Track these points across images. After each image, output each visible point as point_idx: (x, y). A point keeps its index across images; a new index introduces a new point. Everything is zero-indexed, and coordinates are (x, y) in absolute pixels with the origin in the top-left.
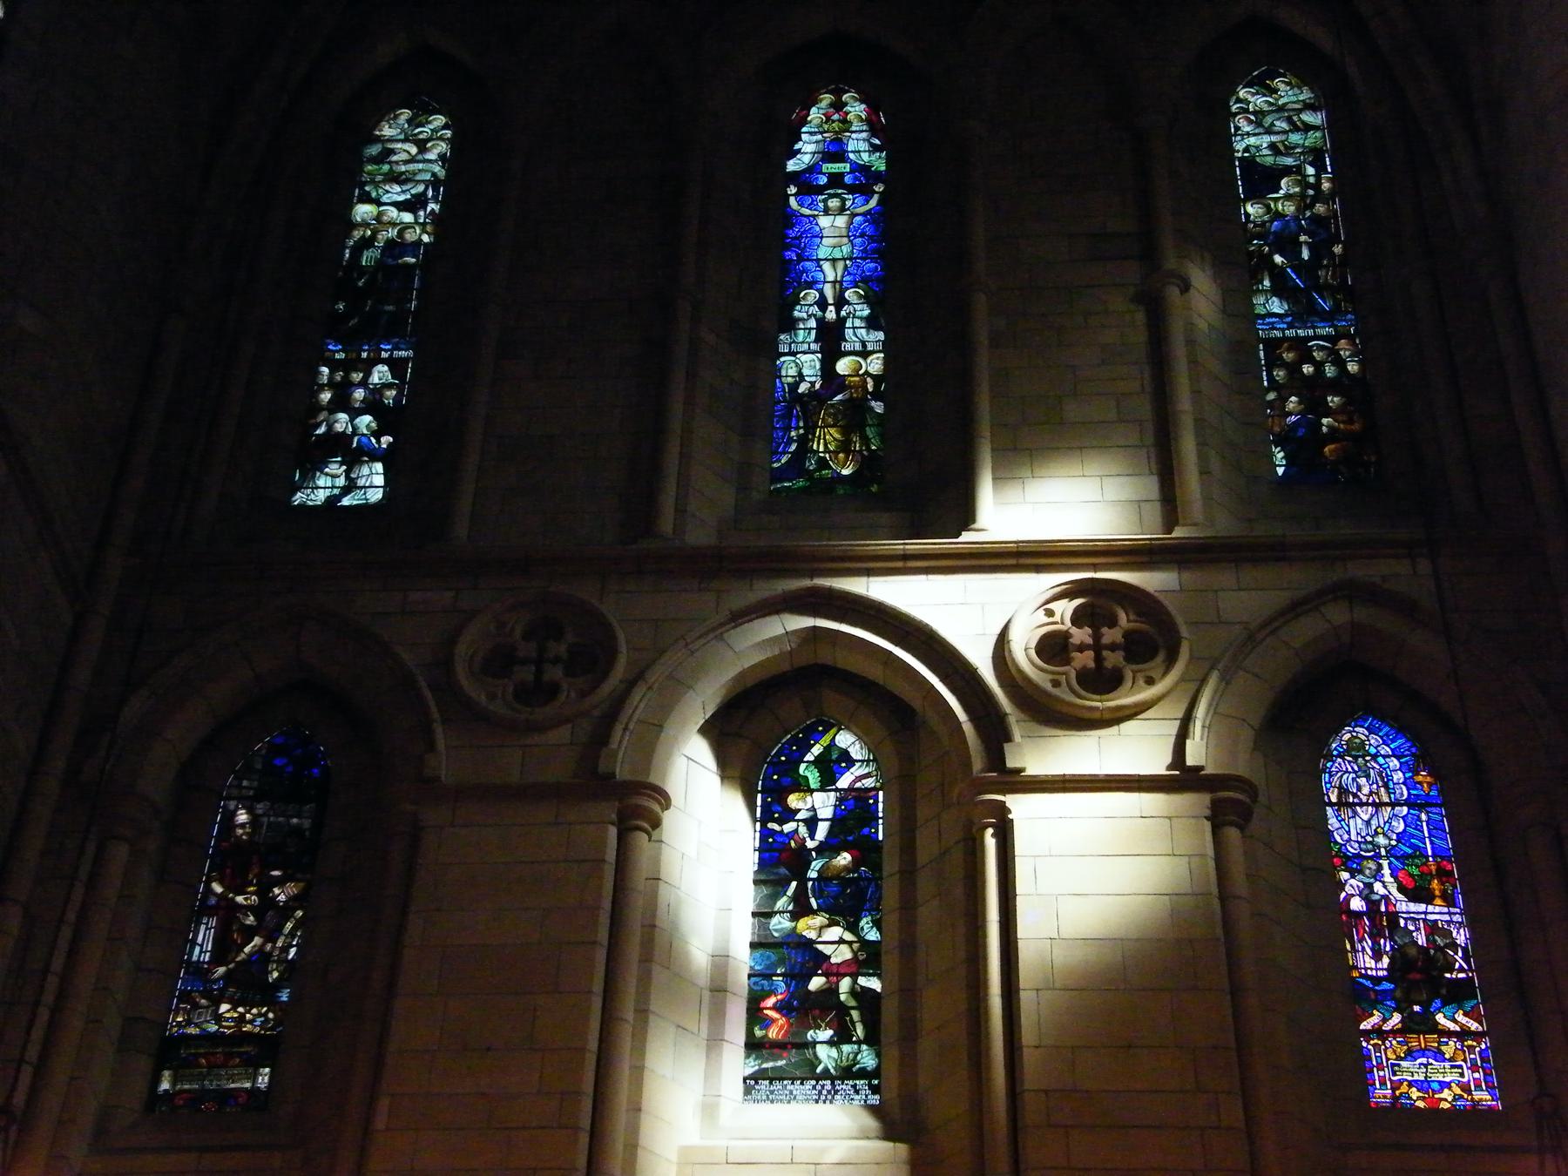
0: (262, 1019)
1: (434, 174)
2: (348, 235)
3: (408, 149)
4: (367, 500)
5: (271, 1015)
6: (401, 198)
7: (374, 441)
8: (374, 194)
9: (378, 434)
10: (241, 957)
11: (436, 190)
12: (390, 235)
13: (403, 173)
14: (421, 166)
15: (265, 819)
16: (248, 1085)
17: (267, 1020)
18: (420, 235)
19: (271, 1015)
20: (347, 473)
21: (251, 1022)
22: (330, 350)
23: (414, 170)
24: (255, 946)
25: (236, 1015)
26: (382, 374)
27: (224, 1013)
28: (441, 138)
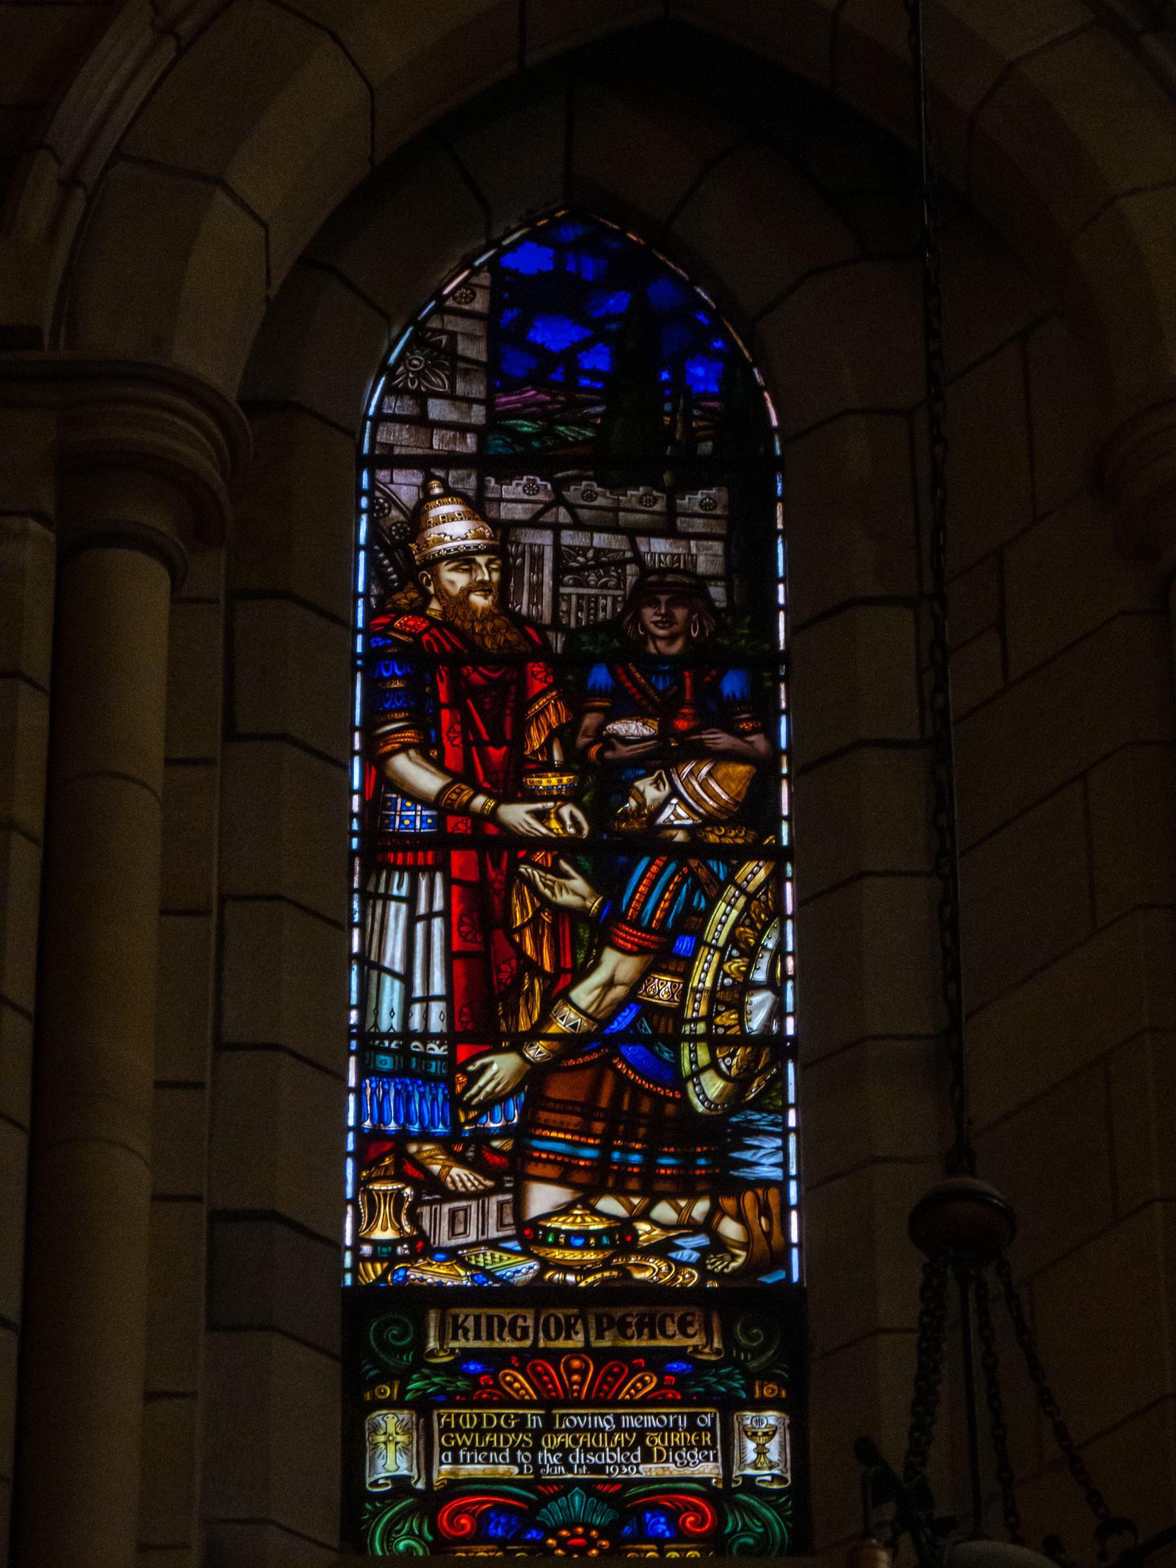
0: (702, 1240)
5: (730, 1229)
10: (565, 1021)
15: (545, 538)
16: (709, 1469)
17: (719, 1245)
19: (730, 1229)
21: (662, 1249)
24: (610, 984)
25: (596, 1225)
27: (547, 1216)
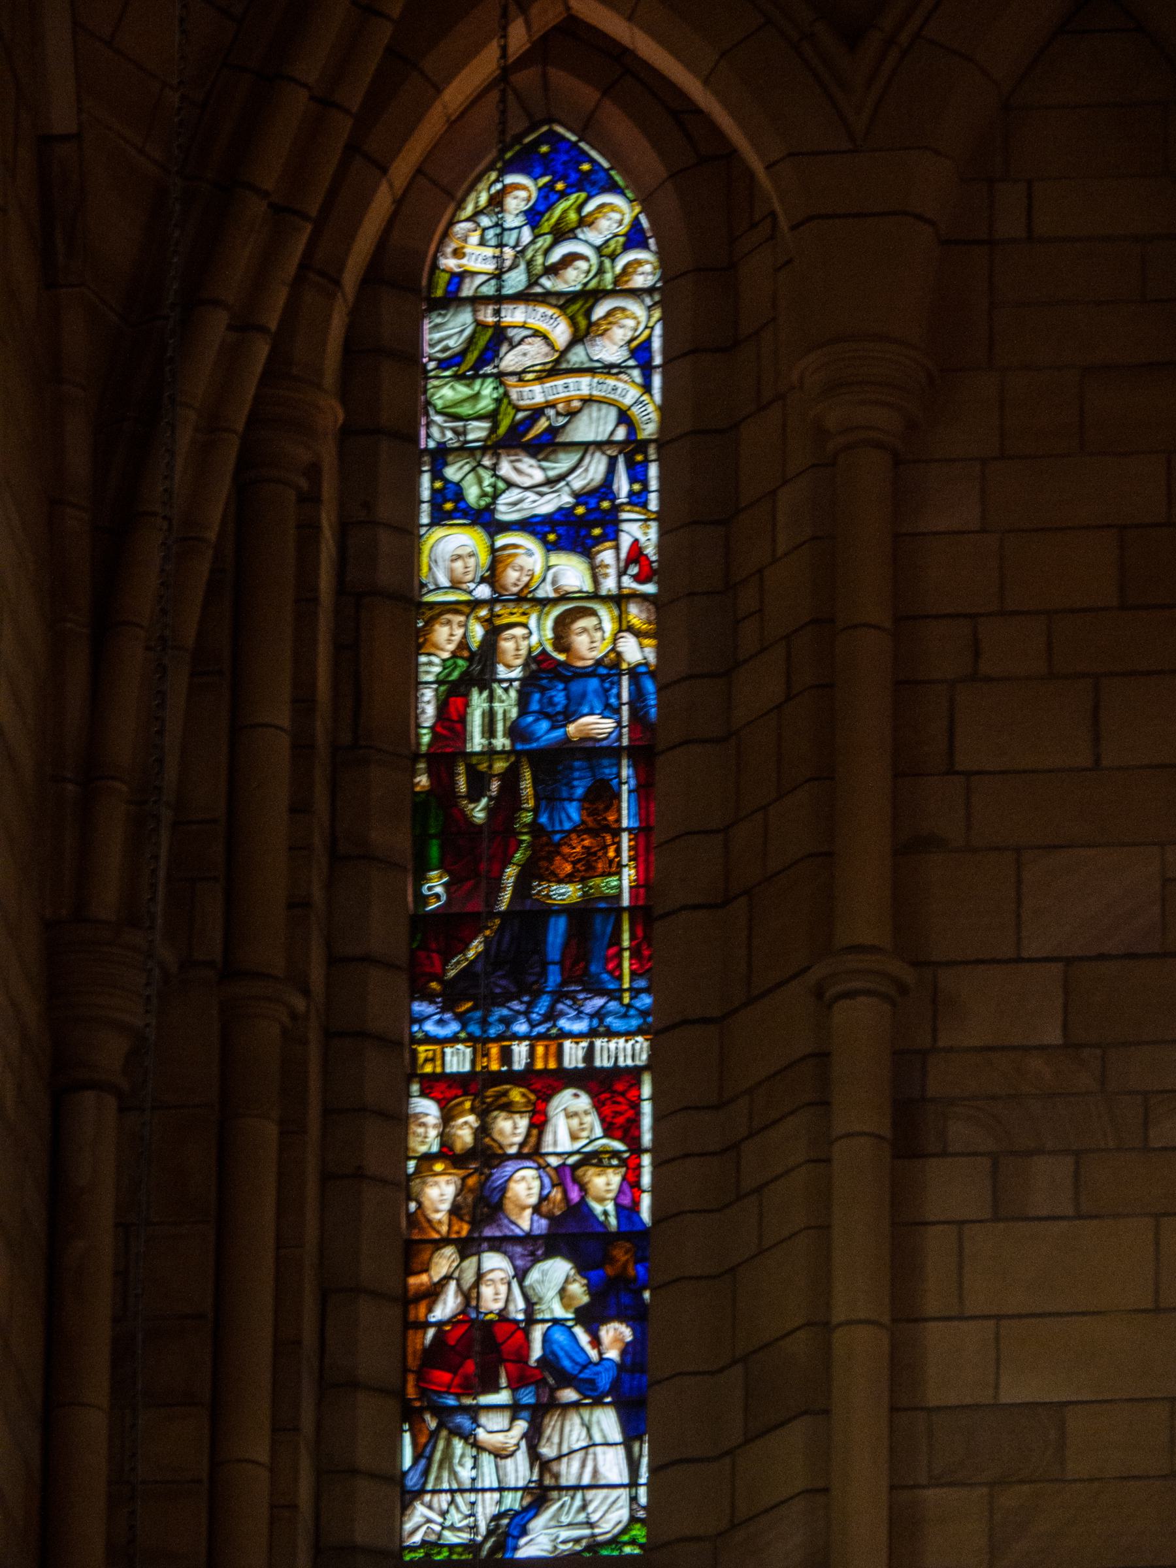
1: (624, 417)
2: (419, 642)
3: (542, 326)
4: (591, 1525)
6: (546, 505)
7: (583, 1338)
8: (472, 494)
9: (590, 1318)
11: (637, 474)
12: (534, 639)
13: (537, 412)
14: (584, 385)
18: (615, 640)
20: (533, 1438)
22: (429, 1039)
23: (568, 401)
26: (575, 1122)
28: (620, 290)
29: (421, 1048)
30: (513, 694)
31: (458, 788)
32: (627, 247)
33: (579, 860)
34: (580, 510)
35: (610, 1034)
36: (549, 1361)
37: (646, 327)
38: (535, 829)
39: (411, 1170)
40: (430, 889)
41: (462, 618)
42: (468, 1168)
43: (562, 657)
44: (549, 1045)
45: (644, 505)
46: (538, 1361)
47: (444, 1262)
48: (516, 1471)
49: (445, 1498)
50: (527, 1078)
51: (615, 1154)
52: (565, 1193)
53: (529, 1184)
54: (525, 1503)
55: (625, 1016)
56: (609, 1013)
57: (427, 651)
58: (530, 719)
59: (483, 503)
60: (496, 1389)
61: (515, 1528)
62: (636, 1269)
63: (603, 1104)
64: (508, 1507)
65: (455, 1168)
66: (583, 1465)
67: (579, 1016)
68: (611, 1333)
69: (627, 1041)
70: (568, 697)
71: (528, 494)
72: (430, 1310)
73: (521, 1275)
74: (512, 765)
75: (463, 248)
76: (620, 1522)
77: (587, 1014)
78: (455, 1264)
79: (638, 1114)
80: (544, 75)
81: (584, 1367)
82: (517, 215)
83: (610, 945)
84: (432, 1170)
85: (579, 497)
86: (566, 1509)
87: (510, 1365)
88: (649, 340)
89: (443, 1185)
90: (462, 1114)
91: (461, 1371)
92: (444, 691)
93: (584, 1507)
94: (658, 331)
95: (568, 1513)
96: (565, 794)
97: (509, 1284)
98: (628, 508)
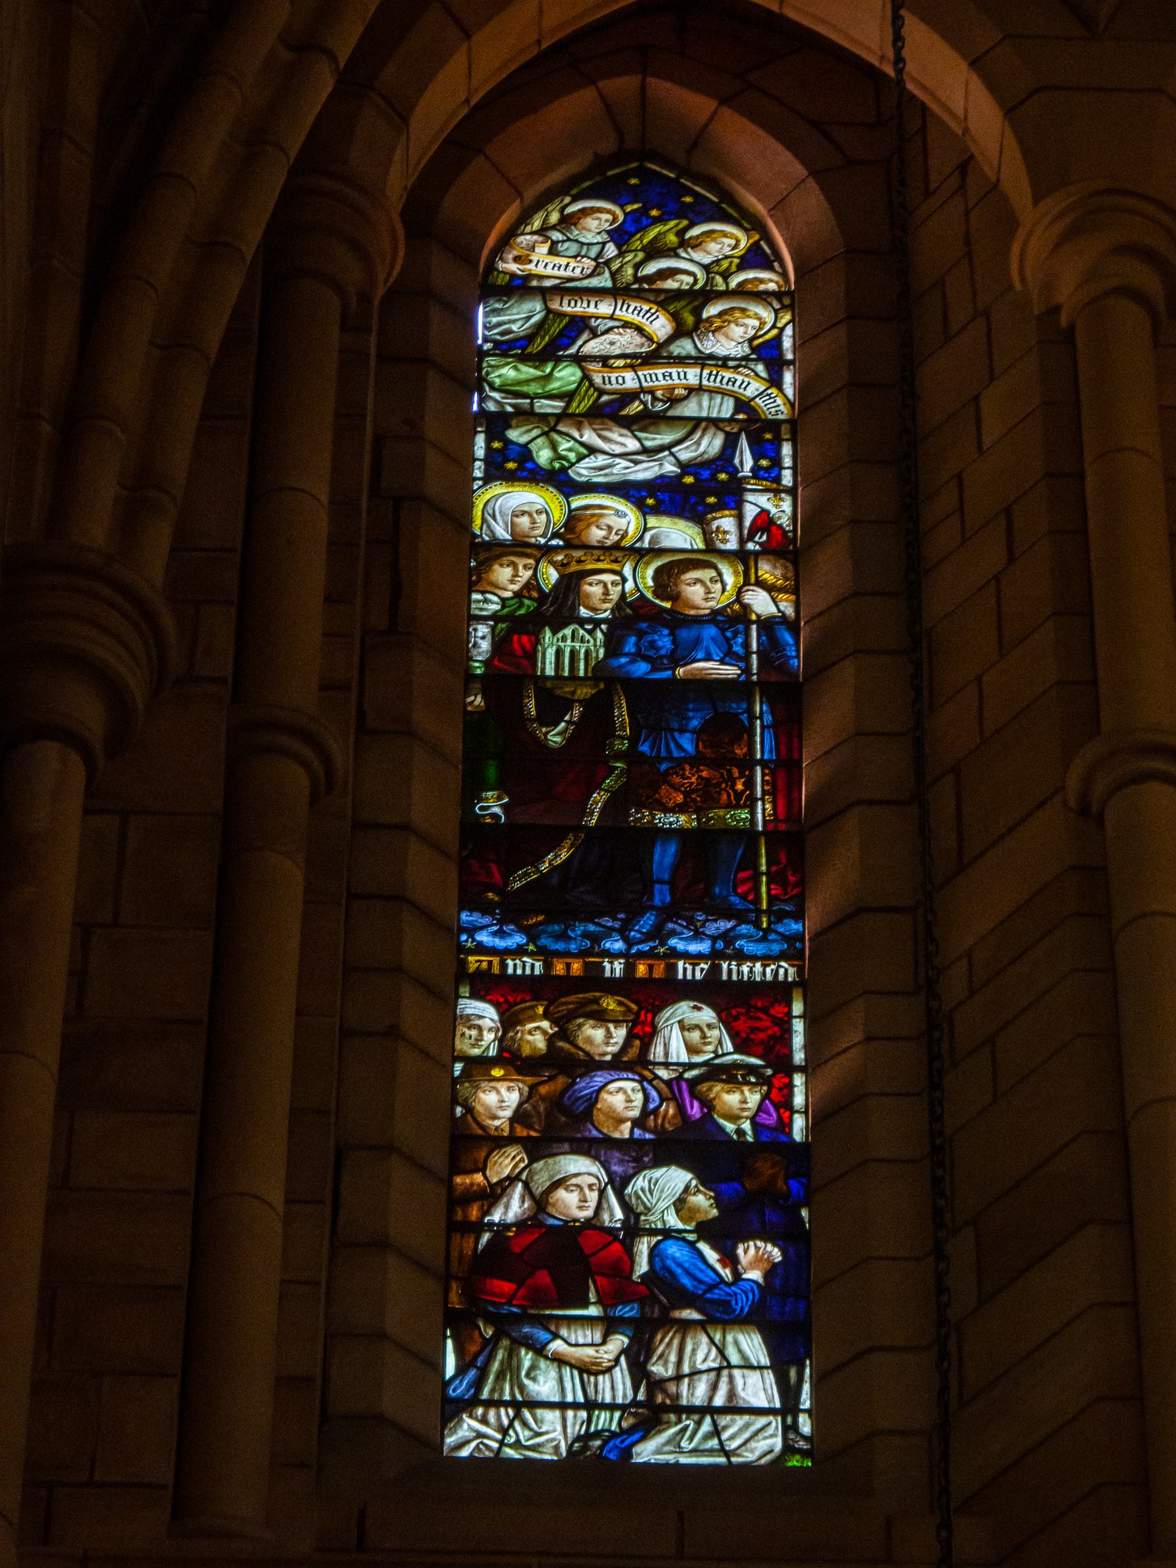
3: (636, 319)
6: (645, 472)
7: (712, 1256)
8: (543, 456)
11: (765, 449)
12: (630, 585)
13: (629, 397)
14: (692, 375)
18: (739, 592)
22: (481, 949)
23: (671, 389)
26: (695, 1036)
29: (471, 959)
30: (599, 635)
31: (526, 706)
32: (741, 268)
33: (693, 791)
34: (689, 480)
35: (741, 957)
36: (661, 1275)
37: (774, 326)
38: (632, 756)
39: (457, 1073)
40: (482, 809)
41: (532, 561)
42: (540, 1076)
43: (668, 605)
44: (653, 965)
45: (778, 479)
46: (642, 1277)
47: (505, 1164)
48: (613, 1388)
49: (506, 1414)
50: (625, 986)
51: (751, 1069)
52: (681, 1109)
53: (628, 1096)
54: (624, 1425)
55: (764, 939)
56: (742, 936)
57: (481, 589)
58: (623, 660)
59: (557, 465)
60: (585, 1304)
61: (610, 1451)
62: (787, 1184)
63: (736, 1018)
64: (600, 1427)
65: (519, 1074)
66: (714, 1387)
67: (698, 936)
68: (752, 1251)
69: (764, 966)
70: (674, 642)
71: (618, 460)
72: (488, 1212)
73: (619, 1184)
74: (600, 692)
75: (528, 255)
76: (771, 1451)
77: (709, 936)
78: (522, 1165)
79: (788, 1032)
80: (643, 87)
81: (711, 1288)
82: (599, 233)
83: (741, 867)
84: (491, 1075)
85: (686, 468)
86: (688, 1433)
87: (599, 1279)
88: (778, 339)
89: (503, 1091)
90: (533, 1019)
91: (530, 1282)
92: (502, 629)
93: (716, 1432)
94: (789, 331)
95: (691, 1438)
96: (675, 725)
97: (602, 1193)
98: (752, 481)
